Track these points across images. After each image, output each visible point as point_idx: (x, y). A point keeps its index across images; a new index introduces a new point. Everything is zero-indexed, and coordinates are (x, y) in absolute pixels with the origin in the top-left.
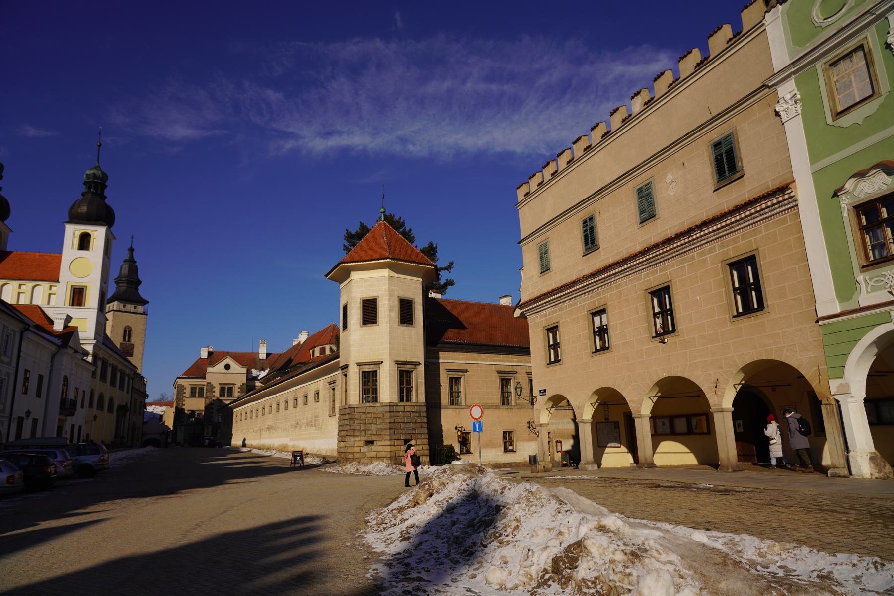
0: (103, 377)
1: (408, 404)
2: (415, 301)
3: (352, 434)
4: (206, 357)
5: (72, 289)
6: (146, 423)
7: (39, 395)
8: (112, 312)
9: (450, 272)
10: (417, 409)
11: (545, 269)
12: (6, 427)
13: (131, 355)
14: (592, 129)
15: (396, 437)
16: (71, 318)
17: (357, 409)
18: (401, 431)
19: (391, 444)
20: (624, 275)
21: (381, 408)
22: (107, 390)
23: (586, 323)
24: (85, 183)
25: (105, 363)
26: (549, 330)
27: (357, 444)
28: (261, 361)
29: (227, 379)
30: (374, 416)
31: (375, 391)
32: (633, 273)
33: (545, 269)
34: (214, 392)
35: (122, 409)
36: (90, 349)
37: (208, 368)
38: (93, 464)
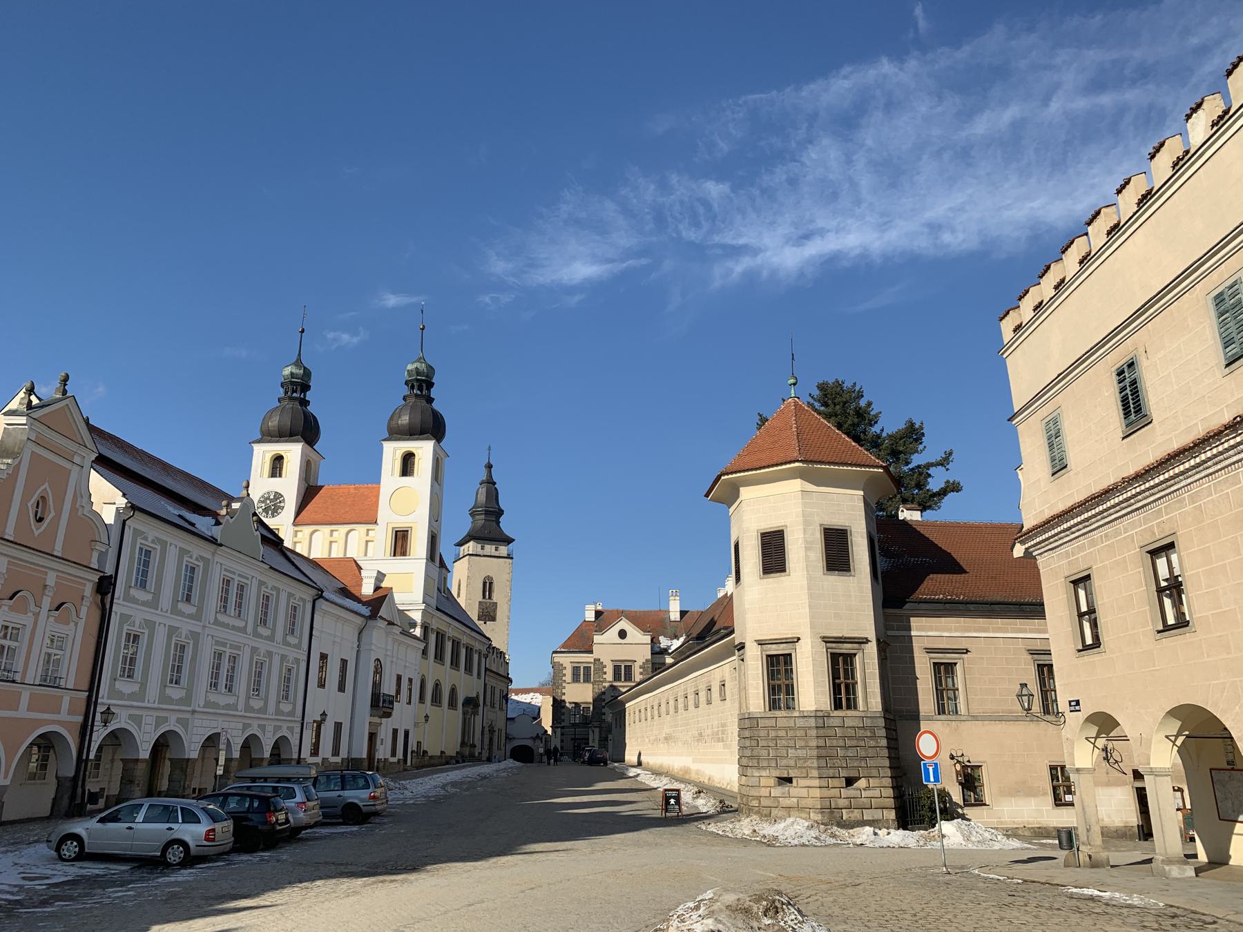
0: (439, 657)
1: (850, 713)
2: (853, 530)
3: (756, 765)
4: (594, 620)
5: (394, 532)
6: (513, 719)
7: (342, 688)
8: (467, 557)
9: (947, 470)
10: (868, 722)
11: (1059, 467)
13: (493, 619)
14: (1119, 192)
15: (831, 772)
16: (385, 575)
17: (762, 720)
18: (838, 763)
19: (822, 785)
20: (1203, 474)
21: (801, 720)
22: (447, 676)
23: (1139, 572)
24: (406, 383)
25: (441, 637)
26: (1075, 583)
27: (766, 779)
28: (672, 624)
29: (623, 653)
30: (791, 733)
31: (790, 690)
32: (1220, 470)
33: (1059, 467)
34: (605, 673)
35: (471, 702)
36: (417, 616)
37: (595, 637)
38: (361, 804)
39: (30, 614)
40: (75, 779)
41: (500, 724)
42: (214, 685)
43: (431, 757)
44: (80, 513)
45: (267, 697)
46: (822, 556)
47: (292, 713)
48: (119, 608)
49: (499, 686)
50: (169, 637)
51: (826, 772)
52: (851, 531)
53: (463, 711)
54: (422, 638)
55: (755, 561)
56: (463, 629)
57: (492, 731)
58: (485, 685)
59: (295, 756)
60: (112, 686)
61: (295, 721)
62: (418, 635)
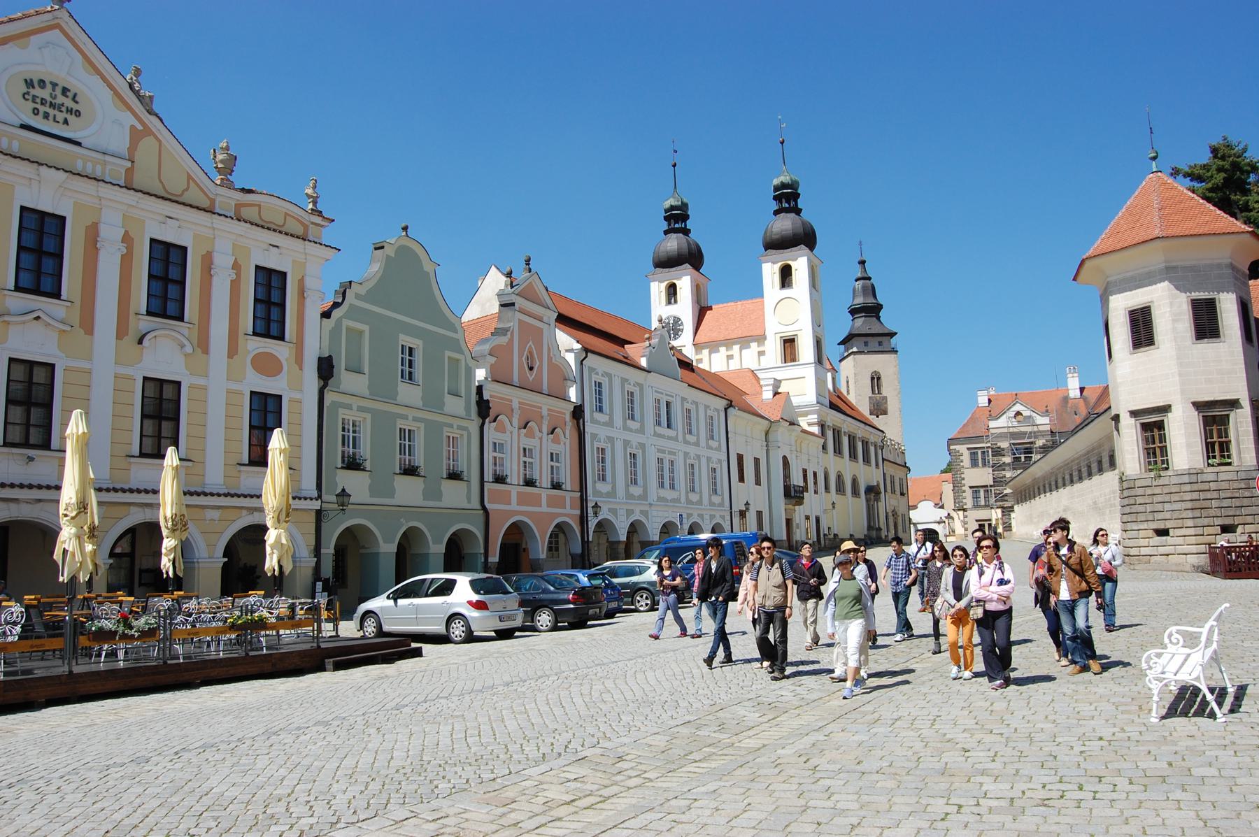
0: (838, 451)
7: (758, 482)
13: (885, 413)
15: (1206, 522)
18: (1212, 512)
25: (837, 434)
31: (1164, 450)
35: (873, 491)
40: (582, 555)
41: (901, 510)
42: (662, 485)
45: (701, 492)
47: (721, 504)
48: (589, 429)
49: (898, 473)
51: (1200, 522)
57: (895, 513)
58: (884, 474)
60: (594, 487)
62: (817, 432)
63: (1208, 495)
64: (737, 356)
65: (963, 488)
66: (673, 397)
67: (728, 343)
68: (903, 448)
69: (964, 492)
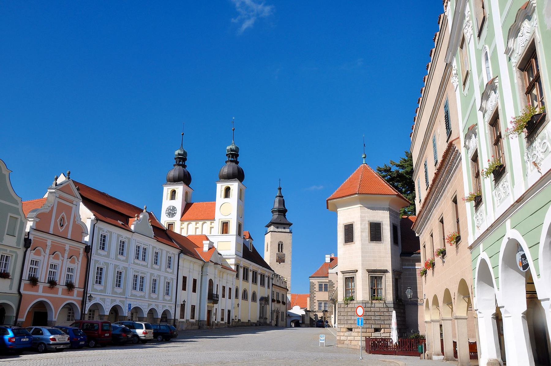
7: (194, 290)
12: (174, 310)
13: (283, 261)
15: (368, 326)
18: (371, 322)
35: (264, 300)
39: (60, 260)
43: (243, 322)
44: (77, 223)
45: (159, 294)
46: (369, 235)
47: (171, 300)
49: (281, 292)
50: (115, 269)
51: (366, 326)
52: (382, 223)
53: (260, 303)
54: (236, 270)
55: (342, 237)
56: (258, 266)
59: (173, 318)
60: (93, 287)
61: (172, 304)
62: (233, 269)
63: (370, 313)
64: (200, 228)
65: (315, 301)
66: (147, 246)
67: (197, 220)
68: (286, 279)
69: (315, 303)
